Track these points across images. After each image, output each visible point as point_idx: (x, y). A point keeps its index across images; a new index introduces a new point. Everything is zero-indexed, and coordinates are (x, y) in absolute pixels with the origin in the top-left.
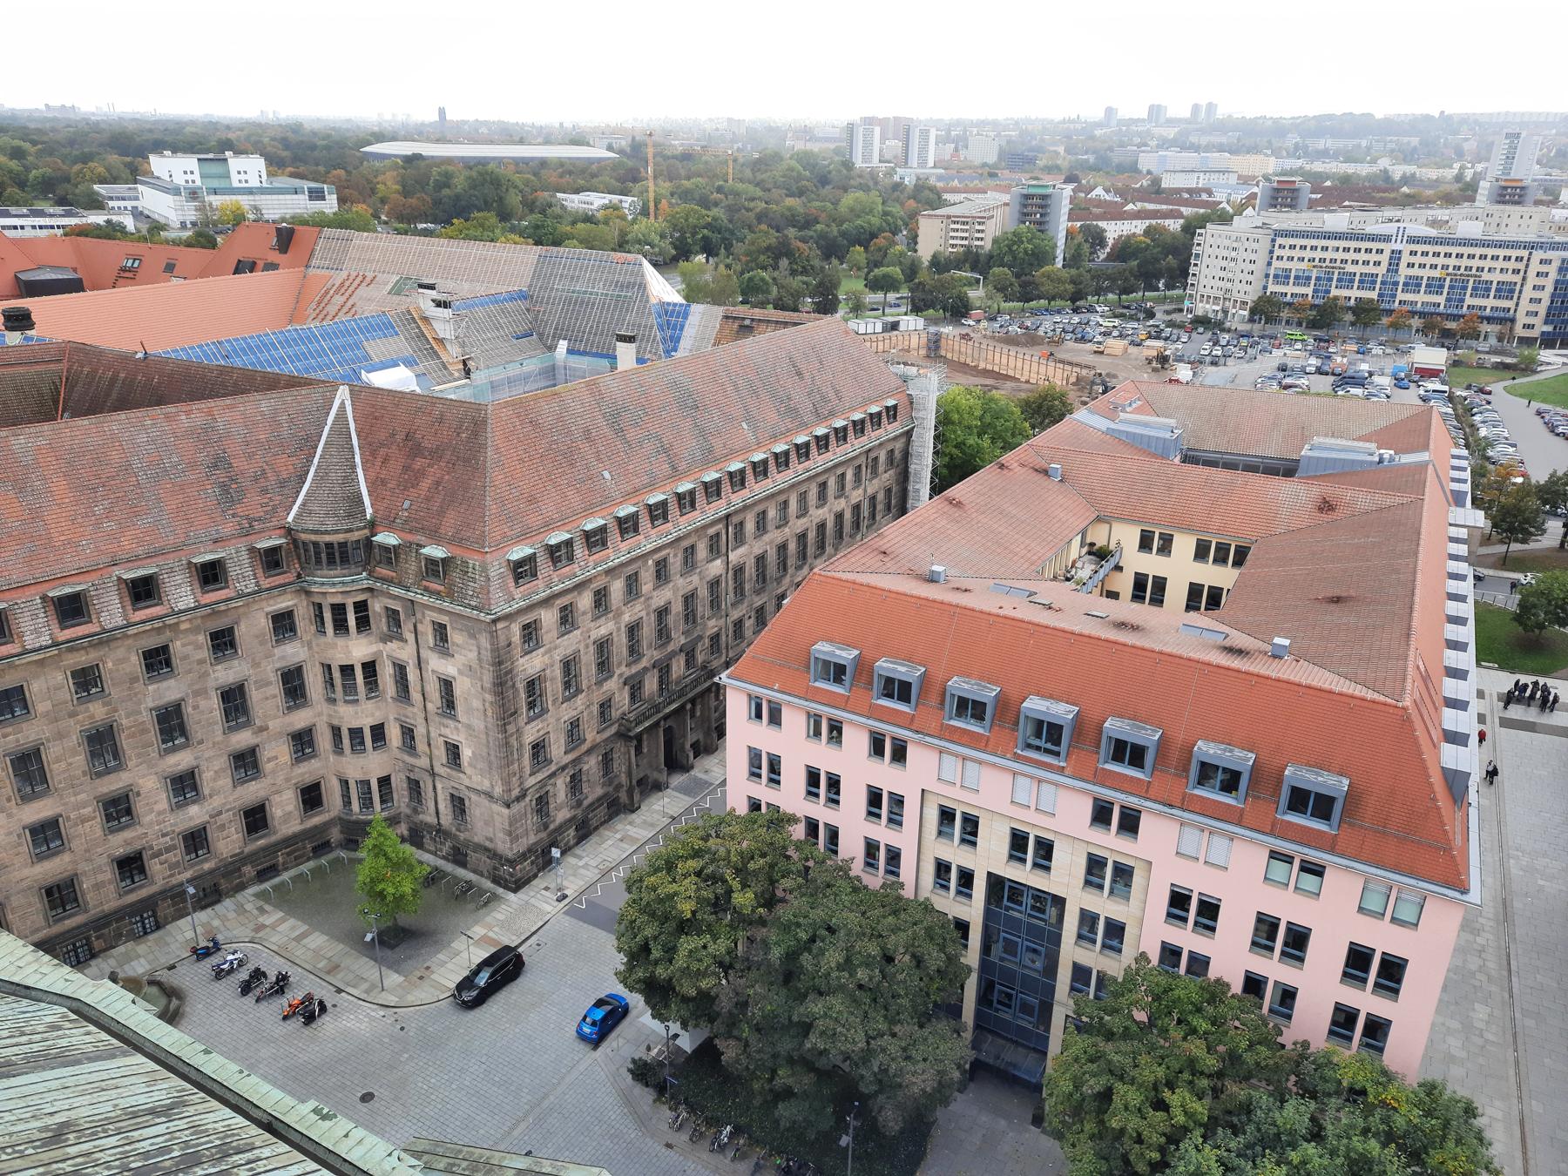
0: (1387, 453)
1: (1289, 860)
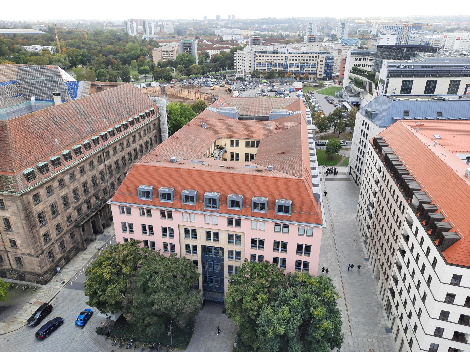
0: (291, 112)
1: (279, 225)
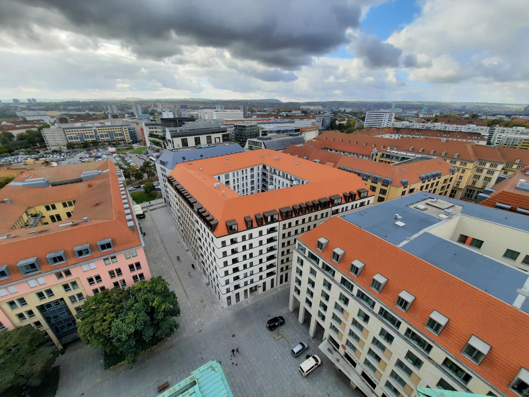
0: (100, 171)
1: (108, 259)
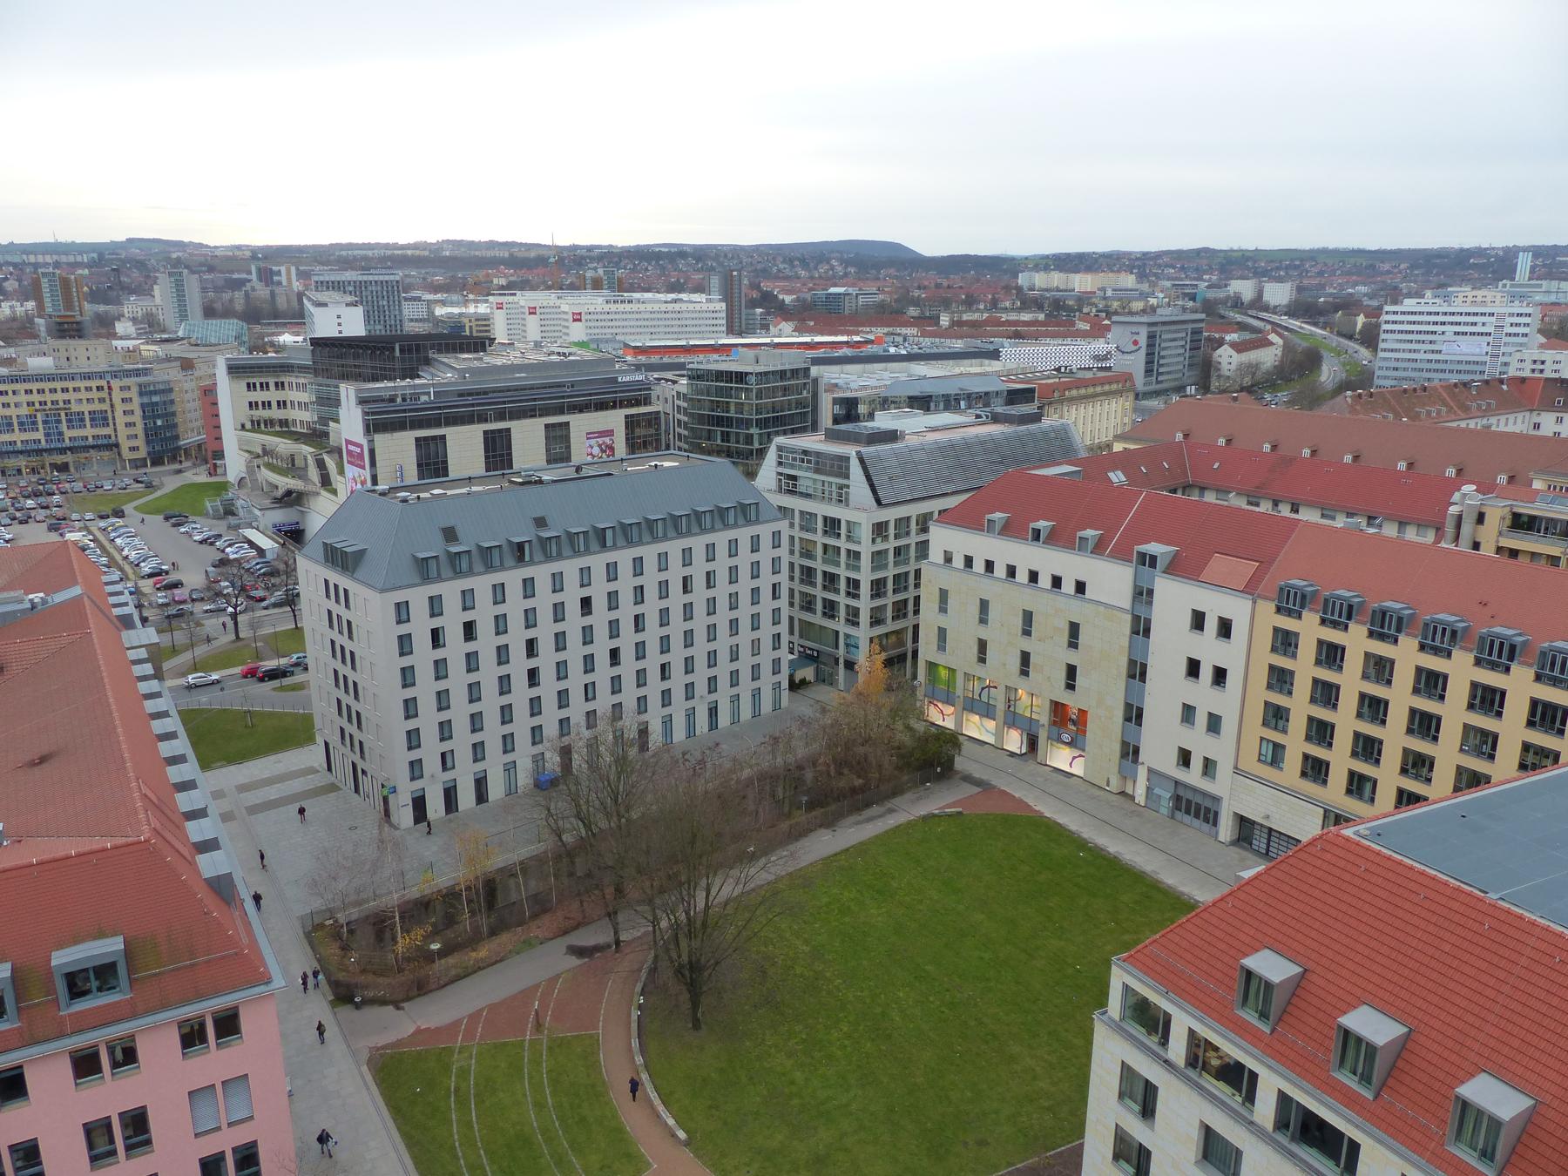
0: (37, 597)
